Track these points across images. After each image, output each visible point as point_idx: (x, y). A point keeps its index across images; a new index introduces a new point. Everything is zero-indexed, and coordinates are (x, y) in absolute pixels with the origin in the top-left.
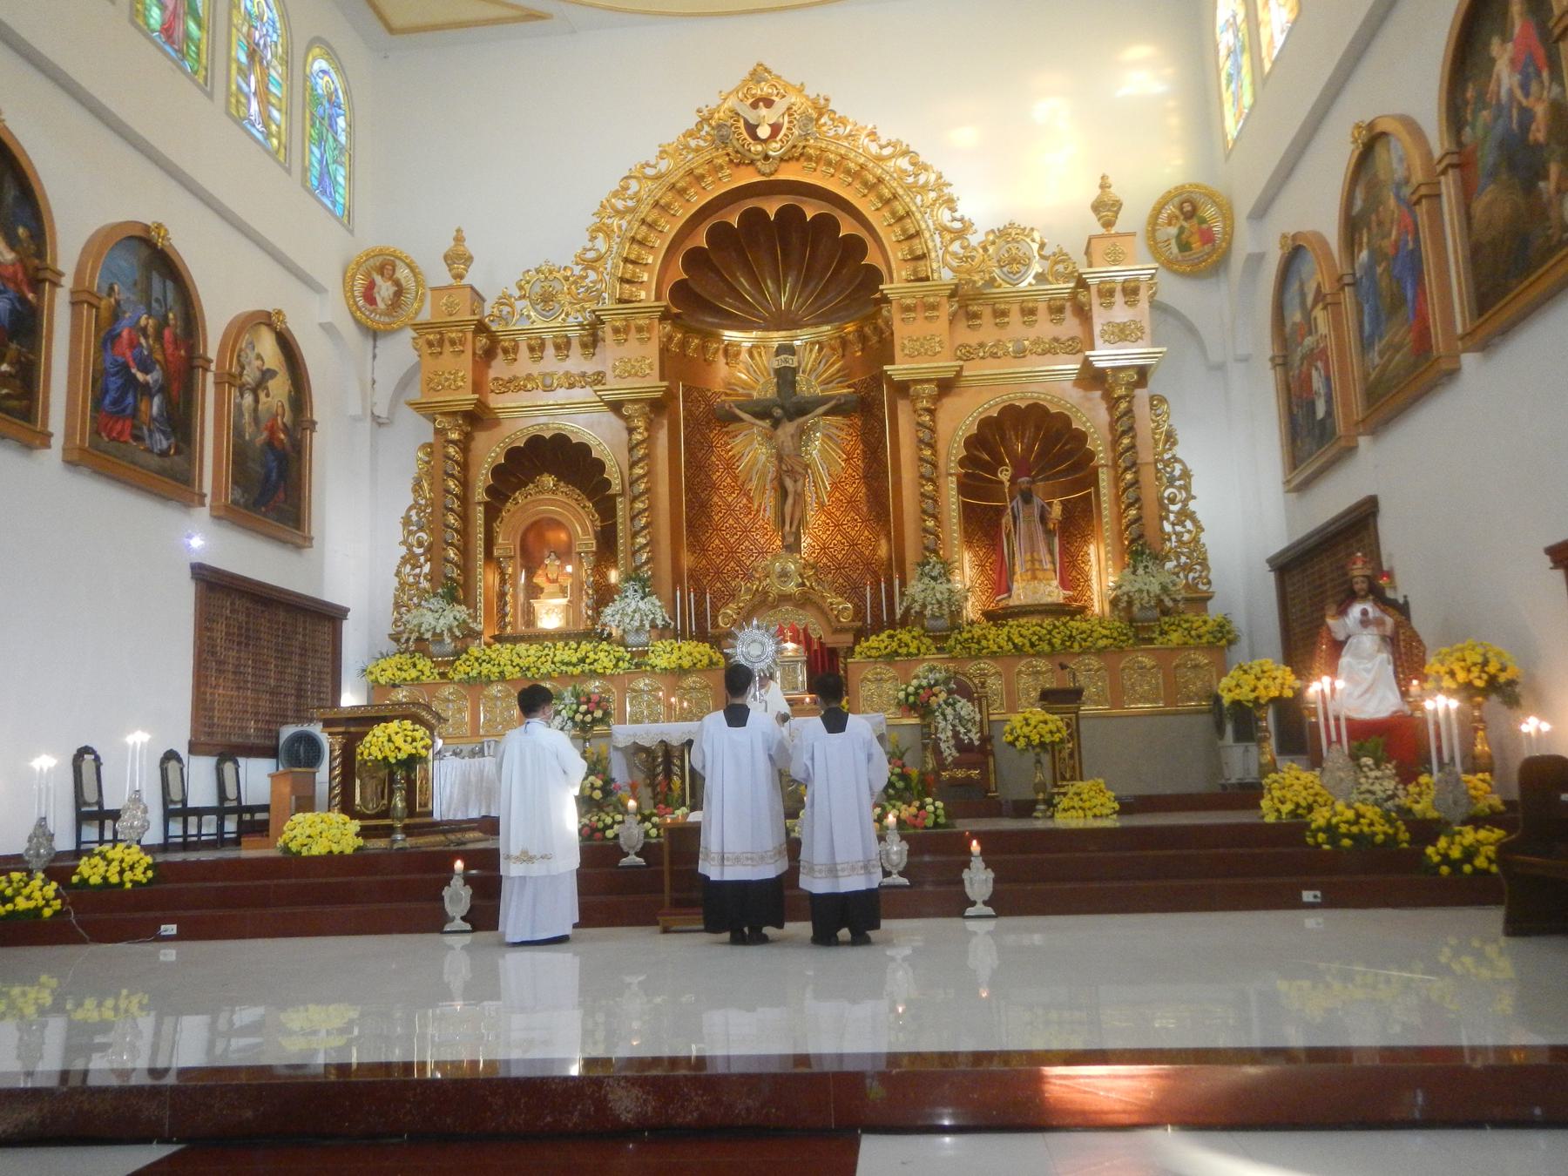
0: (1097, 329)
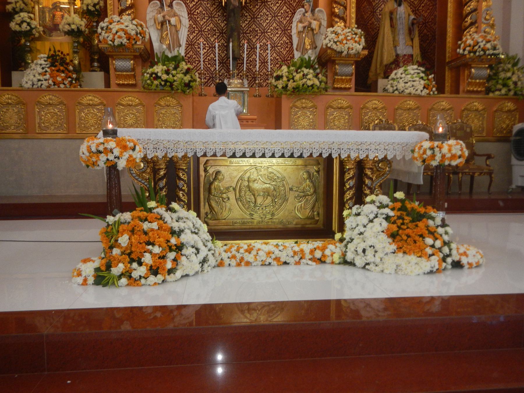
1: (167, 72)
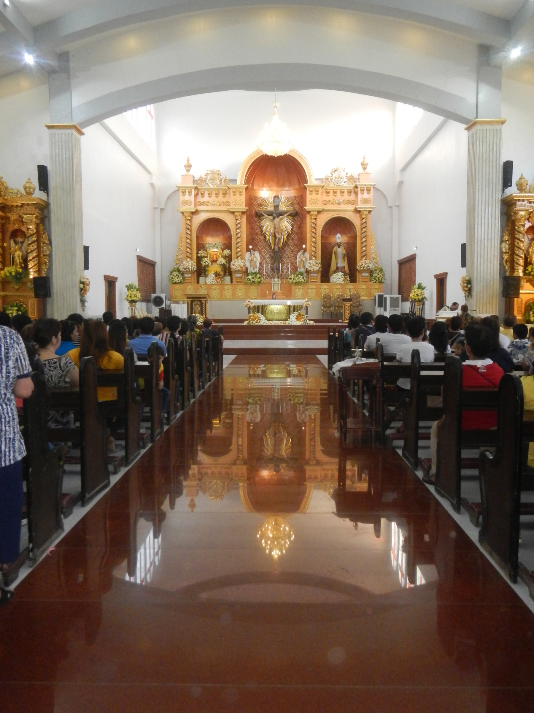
0: (359, 199)
1: (253, 278)
